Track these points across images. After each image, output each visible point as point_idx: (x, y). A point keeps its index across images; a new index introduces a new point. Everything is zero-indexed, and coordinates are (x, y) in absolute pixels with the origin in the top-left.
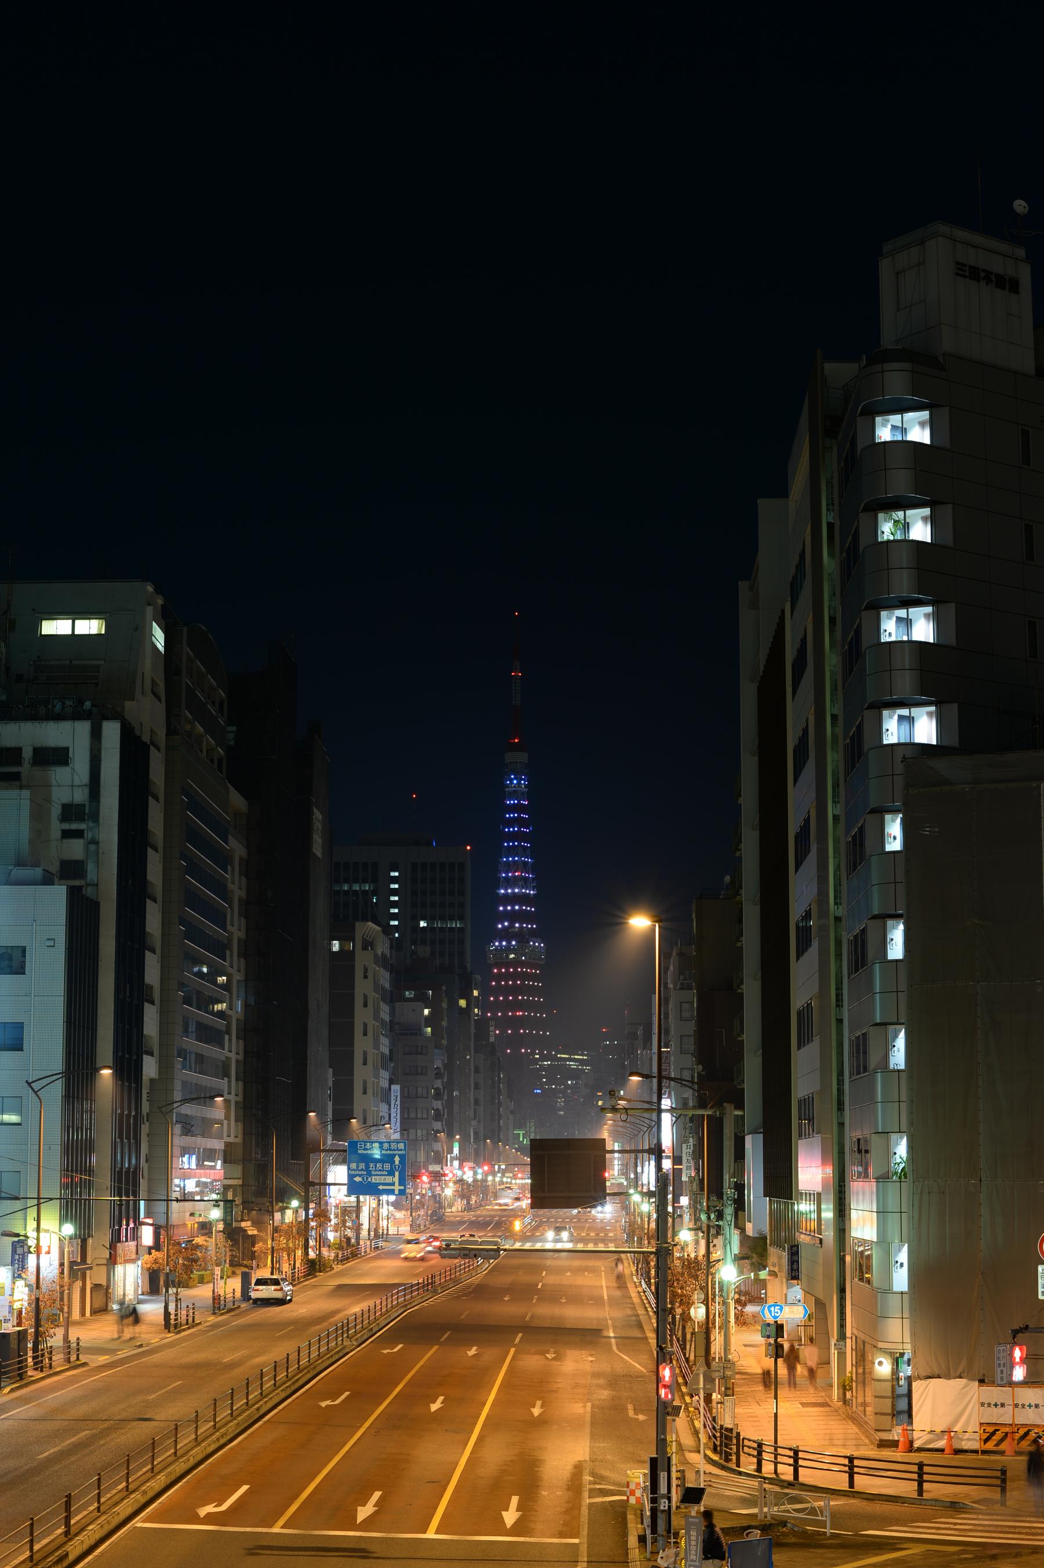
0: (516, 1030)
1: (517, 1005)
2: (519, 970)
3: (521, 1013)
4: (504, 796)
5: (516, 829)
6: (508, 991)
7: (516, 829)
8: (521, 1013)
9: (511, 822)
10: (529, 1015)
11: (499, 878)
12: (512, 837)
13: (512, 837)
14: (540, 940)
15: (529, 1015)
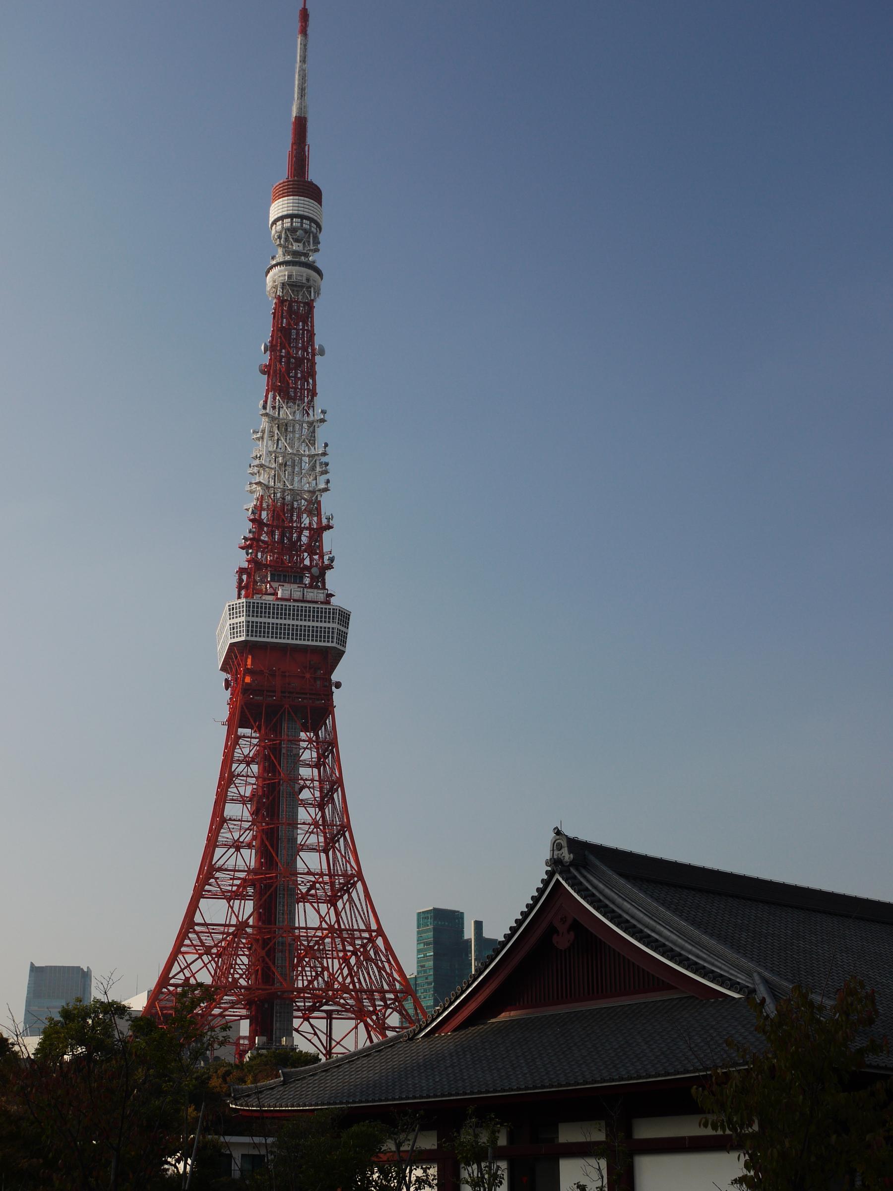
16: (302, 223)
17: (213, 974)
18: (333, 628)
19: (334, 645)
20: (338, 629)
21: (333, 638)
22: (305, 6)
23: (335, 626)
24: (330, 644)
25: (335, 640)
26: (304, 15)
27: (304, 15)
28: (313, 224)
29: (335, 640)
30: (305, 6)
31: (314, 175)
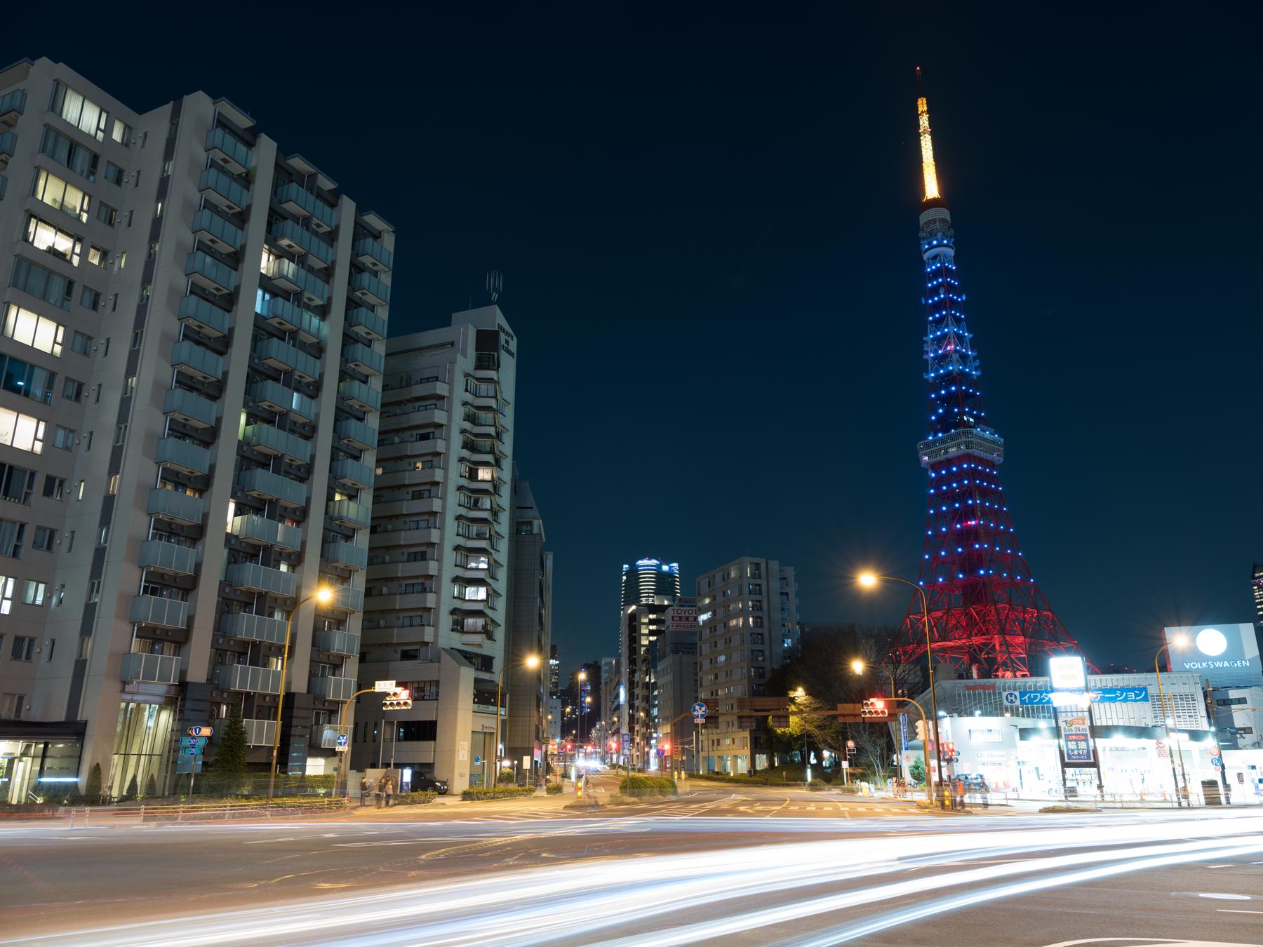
0: (968, 546)
1: (970, 513)
2: (965, 466)
3: (973, 523)
4: (923, 264)
5: (942, 296)
6: (951, 497)
7: (942, 296)
8: (973, 523)
9: (935, 290)
10: (986, 525)
11: (927, 361)
12: (937, 307)
13: (937, 307)
14: (993, 430)
15: (986, 525)
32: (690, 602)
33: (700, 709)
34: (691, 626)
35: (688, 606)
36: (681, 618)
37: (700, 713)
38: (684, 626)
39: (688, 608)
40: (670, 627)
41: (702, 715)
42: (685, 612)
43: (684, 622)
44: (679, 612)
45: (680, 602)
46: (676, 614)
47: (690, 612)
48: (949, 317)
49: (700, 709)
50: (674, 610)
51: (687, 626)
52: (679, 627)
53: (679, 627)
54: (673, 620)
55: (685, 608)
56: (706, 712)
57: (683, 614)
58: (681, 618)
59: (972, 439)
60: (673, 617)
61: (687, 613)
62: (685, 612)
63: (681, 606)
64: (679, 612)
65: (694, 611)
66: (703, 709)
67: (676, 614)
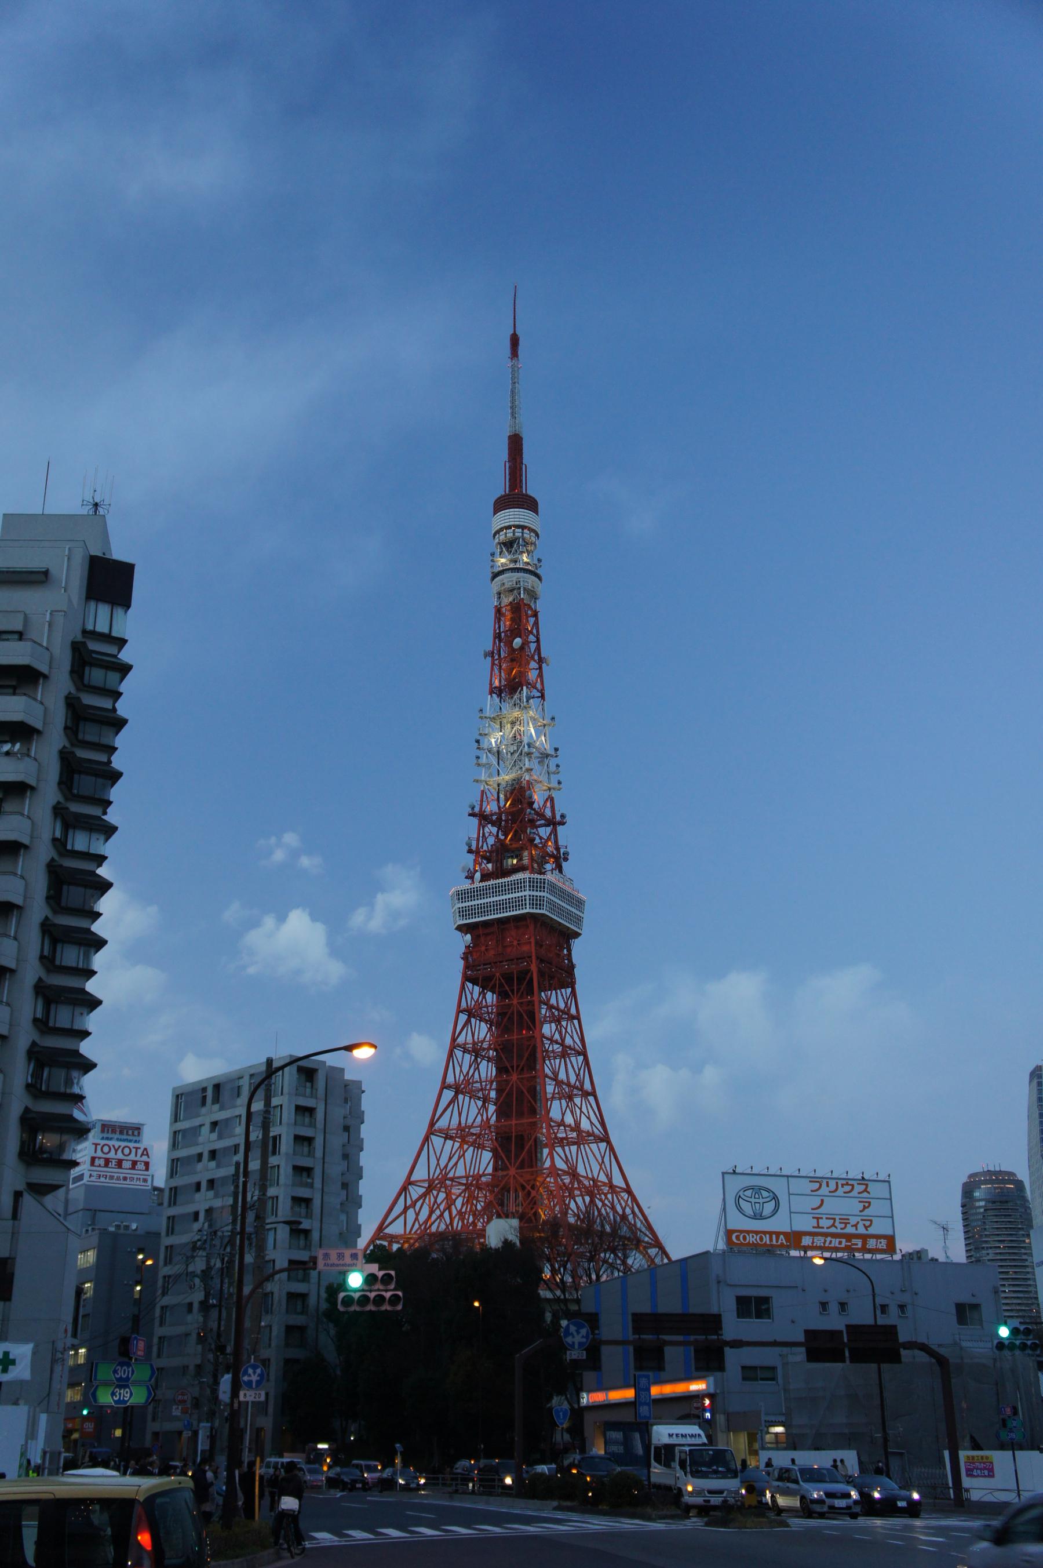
16: (523, 533)
17: (587, 1204)
18: (525, 896)
19: (527, 910)
20: (530, 896)
21: (526, 905)
22: (515, 331)
23: (527, 893)
24: (524, 911)
25: (528, 906)
26: (515, 341)
27: (515, 341)
28: (532, 534)
29: (528, 906)
30: (515, 331)
31: (532, 487)
32: (121, 1133)
33: (578, 1332)
34: (118, 1179)
35: (118, 1139)
36: (107, 1161)
37: (578, 1339)
38: (112, 1177)
39: (123, 1144)
40: (86, 1178)
41: (580, 1344)
42: (116, 1151)
43: (112, 1170)
44: (106, 1149)
45: (103, 1131)
46: (99, 1154)
47: (127, 1151)
48: (525, 688)
49: (578, 1332)
50: (96, 1145)
51: (118, 1179)
52: (102, 1179)
53: (102, 1179)
54: (92, 1163)
55: (111, 1143)
56: (587, 1337)
57: (112, 1155)
58: (107, 1161)
59: (542, 894)
60: (93, 1159)
61: (120, 1151)
62: (116, 1151)
63: (103, 1138)
64: (106, 1149)
65: (134, 1150)
66: (584, 1331)
67: (99, 1154)
